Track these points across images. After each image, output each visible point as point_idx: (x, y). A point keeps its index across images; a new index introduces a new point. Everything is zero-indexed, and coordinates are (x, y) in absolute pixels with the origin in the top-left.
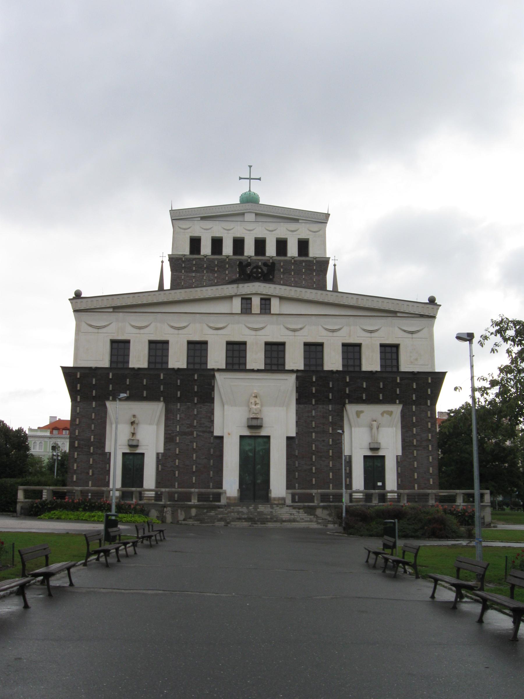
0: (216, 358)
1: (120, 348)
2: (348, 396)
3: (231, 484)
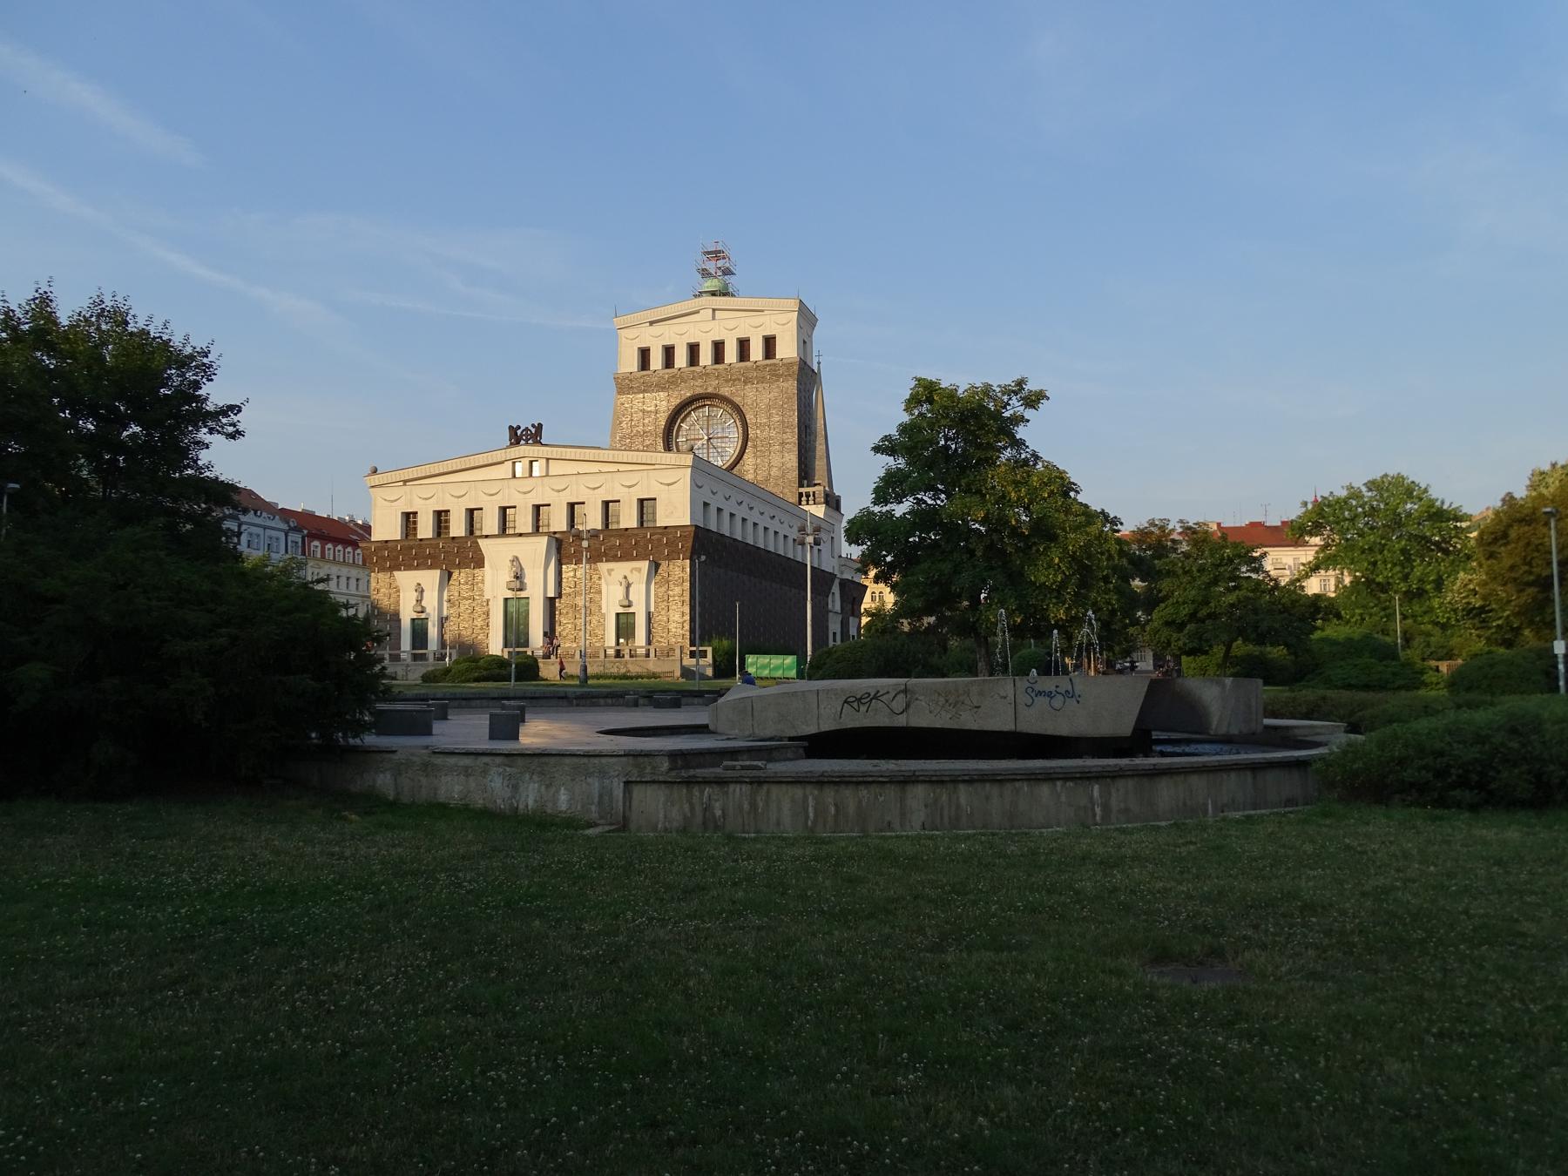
0: (490, 523)
1: (409, 519)
2: (605, 554)
3: (406, 643)
